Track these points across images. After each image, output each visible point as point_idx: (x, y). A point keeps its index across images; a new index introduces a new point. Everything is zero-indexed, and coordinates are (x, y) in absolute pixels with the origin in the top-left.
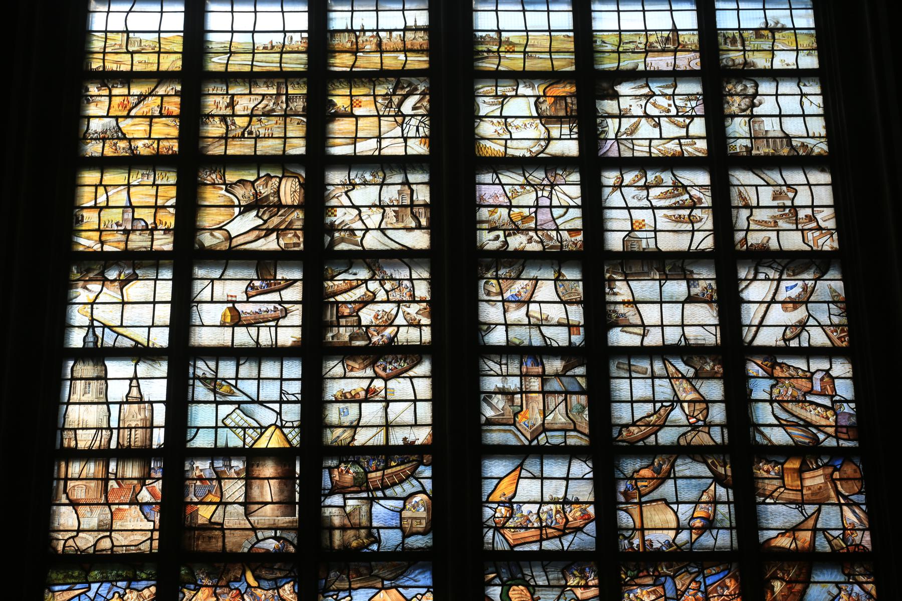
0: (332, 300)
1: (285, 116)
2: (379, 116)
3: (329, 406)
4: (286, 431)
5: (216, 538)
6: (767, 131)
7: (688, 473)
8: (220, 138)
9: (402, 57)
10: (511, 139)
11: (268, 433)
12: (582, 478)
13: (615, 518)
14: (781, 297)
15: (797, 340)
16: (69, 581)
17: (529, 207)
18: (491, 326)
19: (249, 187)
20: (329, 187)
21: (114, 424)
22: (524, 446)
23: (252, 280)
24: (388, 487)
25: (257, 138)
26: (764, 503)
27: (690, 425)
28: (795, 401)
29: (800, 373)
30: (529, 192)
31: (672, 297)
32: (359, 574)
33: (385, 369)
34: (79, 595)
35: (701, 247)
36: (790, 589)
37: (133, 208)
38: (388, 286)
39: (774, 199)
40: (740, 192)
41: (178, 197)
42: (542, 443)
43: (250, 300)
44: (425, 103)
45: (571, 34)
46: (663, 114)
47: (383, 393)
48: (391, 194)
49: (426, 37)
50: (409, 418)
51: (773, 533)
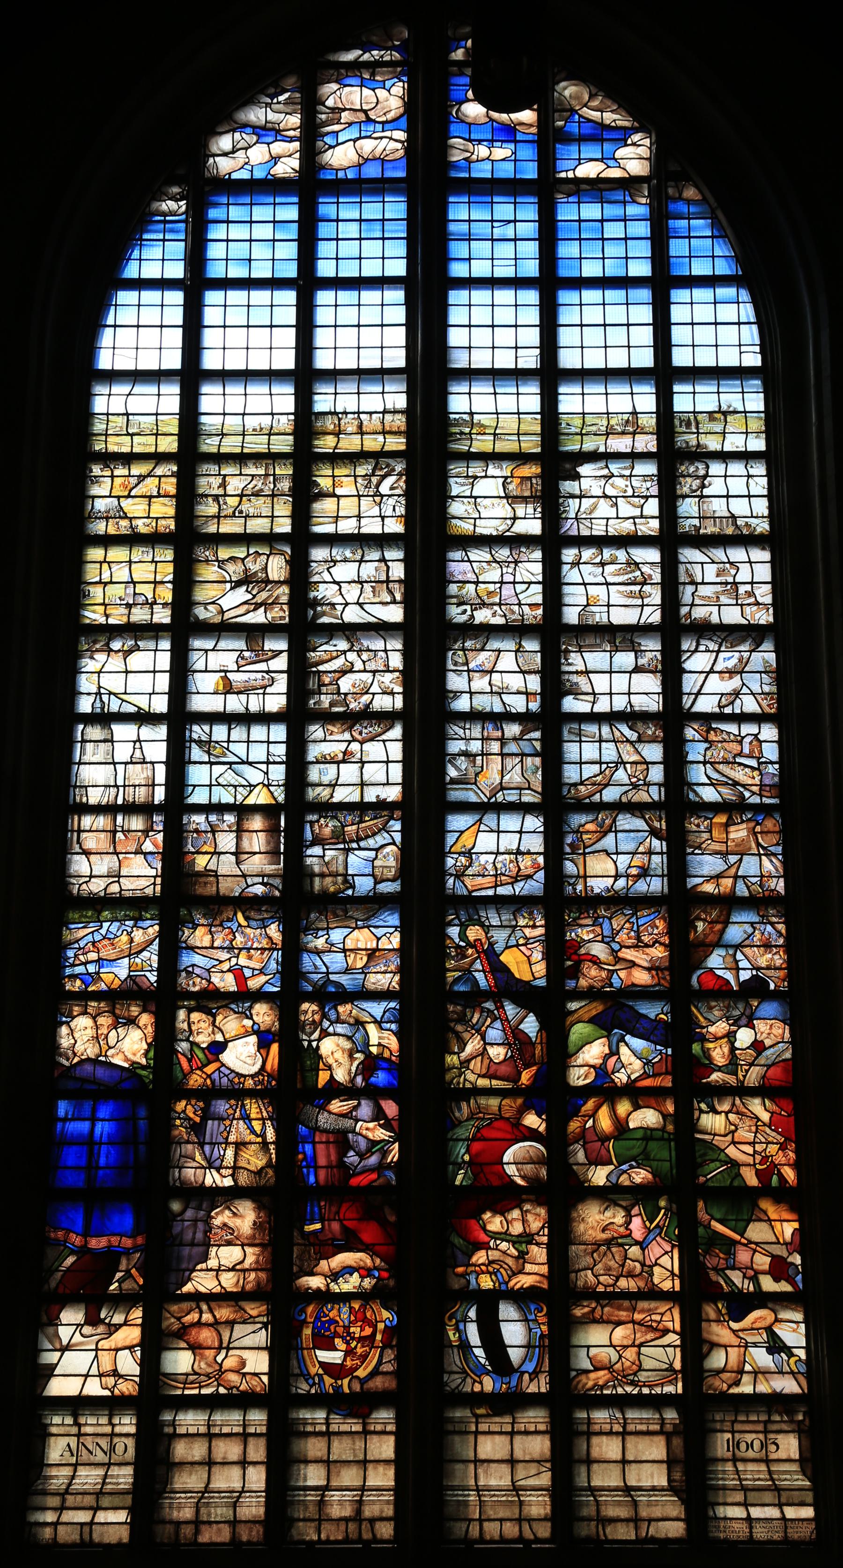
1: (273, 496)
2: (359, 496)
3: (311, 767)
4: (272, 788)
5: (211, 883)
7: (627, 827)
8: (213, 517)
9: (381, 438)
12: (534, 832)
13: (561, 866)
15: (730, 707)
17: (495, 583)
18: (457, 694)
19: (240, 564)
21: (120, 782)
23: (242, 651)
24: (362, 839)
25: (247, 517)
26: (693, 853)
27: (632, 784)
28: (726, 762)
29: (732, 737)
32: (336, 915)
33: (361, 733)
34: (92, 932)
35: (650, 621)
36: (711, 928)
37: (134, 583)
38: (365, 656)
39: (718, 576)
41: (175, 573)
42: (499, 800)
44: (402, 484)
45: (539, 417)
47: (359, 755)
48: (369, 570)
51: (700, 880)
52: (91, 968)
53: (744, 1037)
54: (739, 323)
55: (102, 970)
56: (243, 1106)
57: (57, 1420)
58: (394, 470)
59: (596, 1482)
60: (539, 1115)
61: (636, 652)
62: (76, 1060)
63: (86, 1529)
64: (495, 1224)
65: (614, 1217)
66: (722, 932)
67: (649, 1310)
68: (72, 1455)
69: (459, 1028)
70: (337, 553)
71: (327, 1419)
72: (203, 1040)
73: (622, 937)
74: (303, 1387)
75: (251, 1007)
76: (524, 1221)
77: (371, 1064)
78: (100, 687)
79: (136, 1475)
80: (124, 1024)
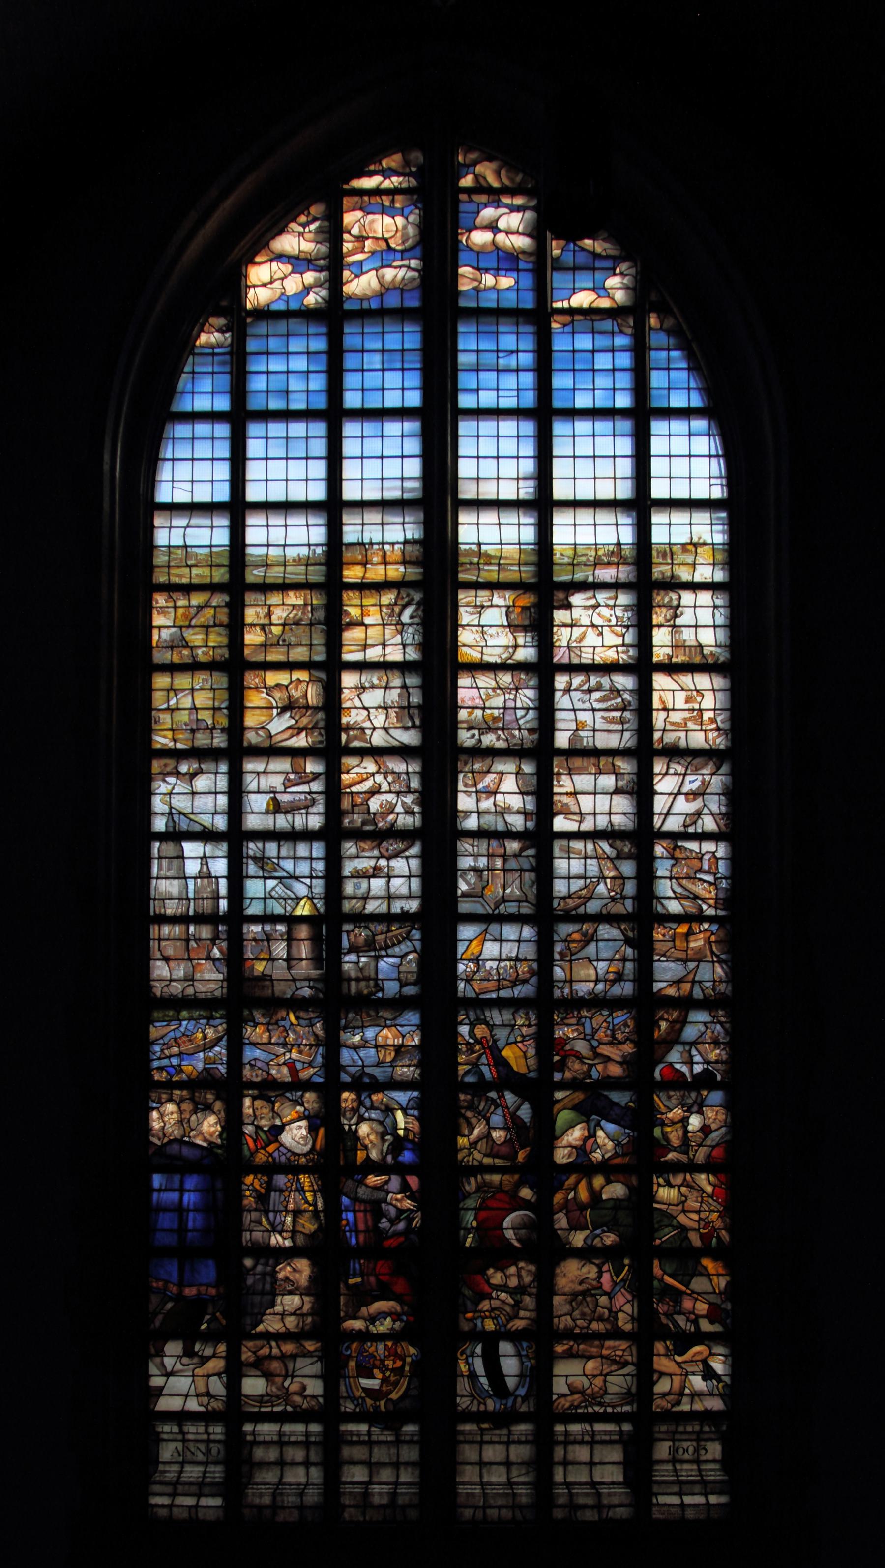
0: (348, 790)
2: (384, 625)
4: (315, 901)
6: (685, 641)
7: (606, 936)
8: (261, 645)
10: (486, 646)
11: (302, 903)
12: (530, 941)
14: (685, 790)
15: (693, 827)
16: (166, 1019)
17: (498, 708)
18: (467, 813)
19: (285, 691)
20: (344, 690)
21: (191, 895)
22: (489, 914)
23: (287, 773)
26: (659, 960)
27: (611, 897)
28: (688, 877)
30: (498, 695)
31: (603, 789)
32: (369, 1016)
33: (387, 850)
34: (174, 1030)
35: (628, 745)
37: (196, 709)
39: (687, 702)
40: (661, 697)
42: (502, 912)
43: (289, 790)
44: (420, 613)
46: (606, 624)
47: (386, 869)
49: (422, 550)
50: (404, 891)
51: (663, 985)
52: (175, 1061)
53: (695, 1122)
54: (710, 456)
55: (184, 1063)
56: (298, 1180)
57: (167, 1429)
58: (413, 599)
59: (570, 1479)
60: (532, 1189)
61: (616, 774)
62: (166, 1140)
63: (193, 1510)
64: (497, 1278)
65: (589, 1273)
66: (681, 1030)
67: (614, 1347)
68: (180, 1455)
69: (469, 1114)
70: (367, 678)
71: (369, 1431)
72: (265, 1123)
73: (601, 1034)
74: (349, 1407)
75: (302, 1096)
76: (519, 1276)
77: (398, 1145)
78: (171, 808)
79: (227, 1471)
80: (202, 1110)
